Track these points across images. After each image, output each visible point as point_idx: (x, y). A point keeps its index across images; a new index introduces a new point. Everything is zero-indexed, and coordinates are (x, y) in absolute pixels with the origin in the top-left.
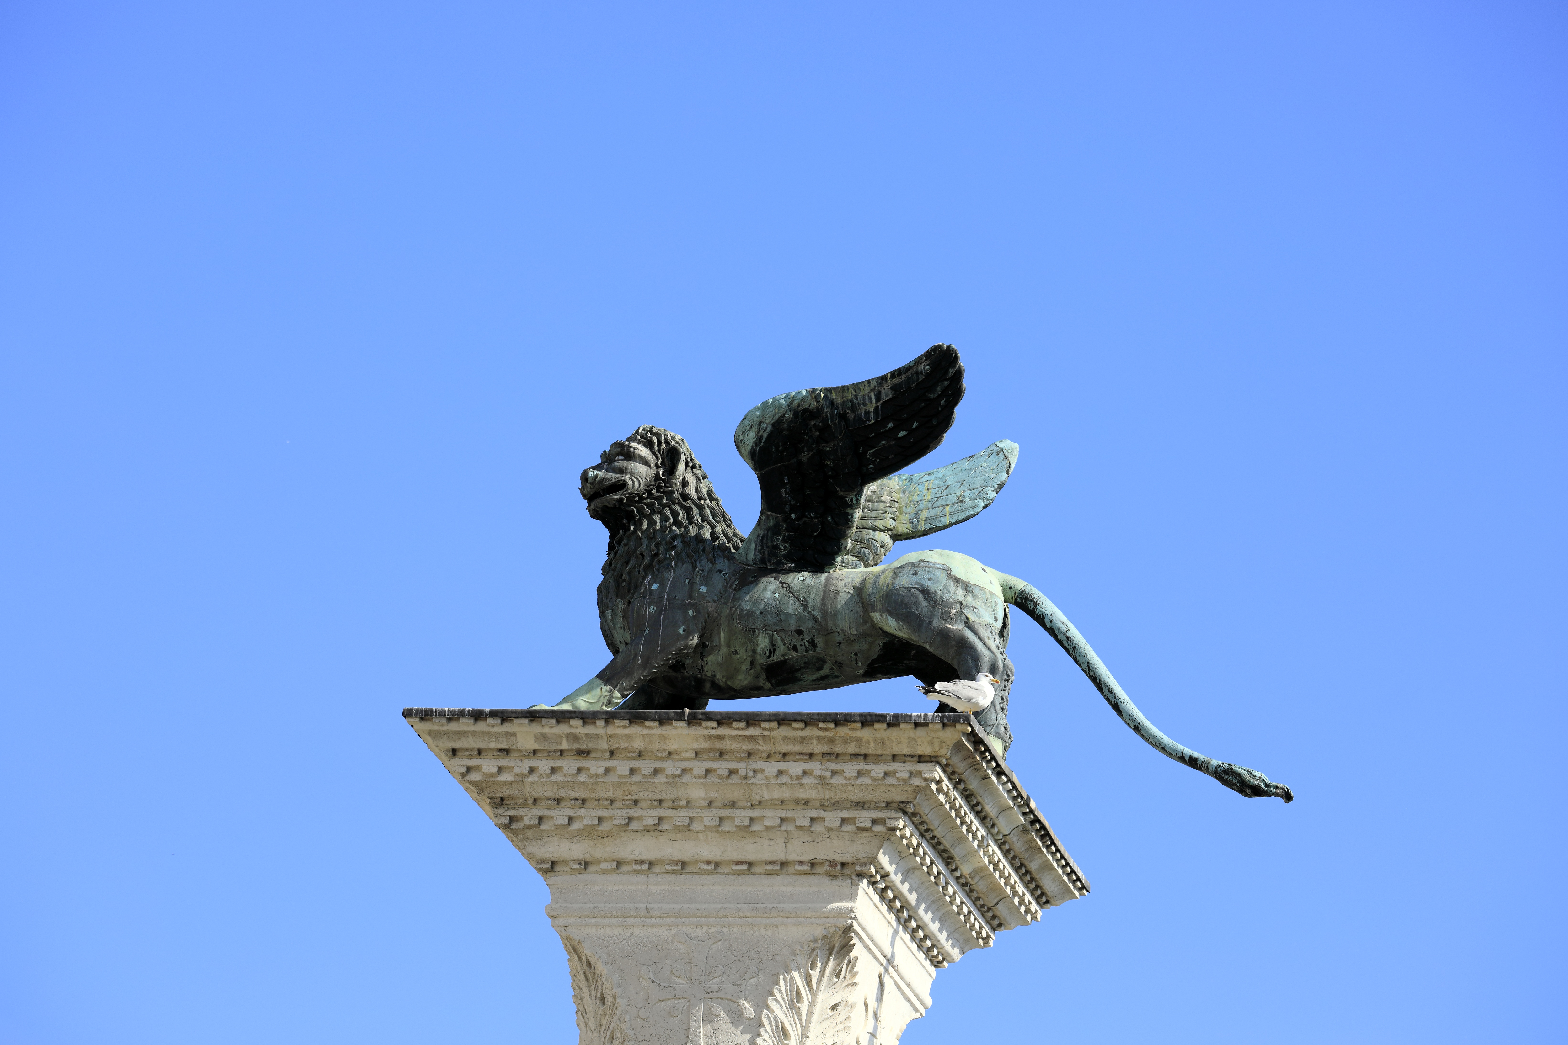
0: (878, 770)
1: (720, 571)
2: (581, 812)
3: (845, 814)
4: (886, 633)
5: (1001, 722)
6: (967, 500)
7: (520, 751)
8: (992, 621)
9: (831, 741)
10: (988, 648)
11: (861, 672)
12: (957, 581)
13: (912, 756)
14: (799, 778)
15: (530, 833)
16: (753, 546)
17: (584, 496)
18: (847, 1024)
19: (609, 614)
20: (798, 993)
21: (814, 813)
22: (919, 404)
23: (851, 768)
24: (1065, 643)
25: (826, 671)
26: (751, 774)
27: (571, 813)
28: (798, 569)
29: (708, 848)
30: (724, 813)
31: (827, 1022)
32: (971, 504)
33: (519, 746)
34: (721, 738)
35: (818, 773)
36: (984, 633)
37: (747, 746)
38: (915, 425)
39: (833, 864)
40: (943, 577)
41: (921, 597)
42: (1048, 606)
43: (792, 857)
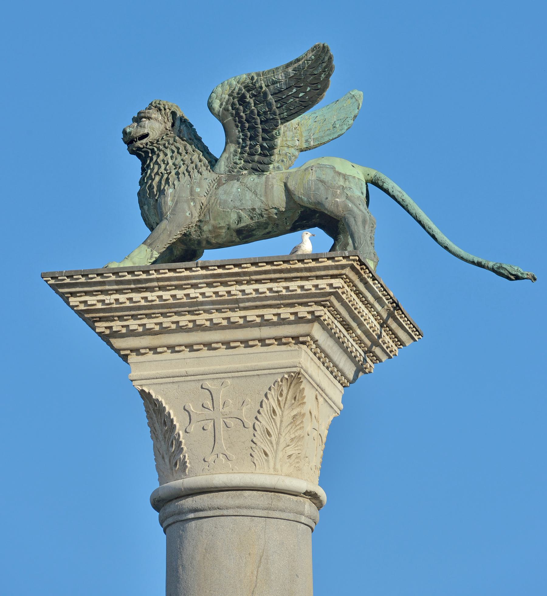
1: (206, 179)
4: (302, 206)
5: (372, 251)
6: (337, 126)
8: (361, 195)
10: (360, 210)
11: (289, 228)
12: (339, 174)
17: (125, 143)
18: (301, 425)
19: (146, 207)
20: (274, 411)
24: (402, 203)
25: (269, 229)
28: (250, 174)
31: (291, 425)
32: (340, 128)
36: (358, 202)
38: (308, 89)
40: (331, 173)
41: (320, 185)
42: (390, 184)
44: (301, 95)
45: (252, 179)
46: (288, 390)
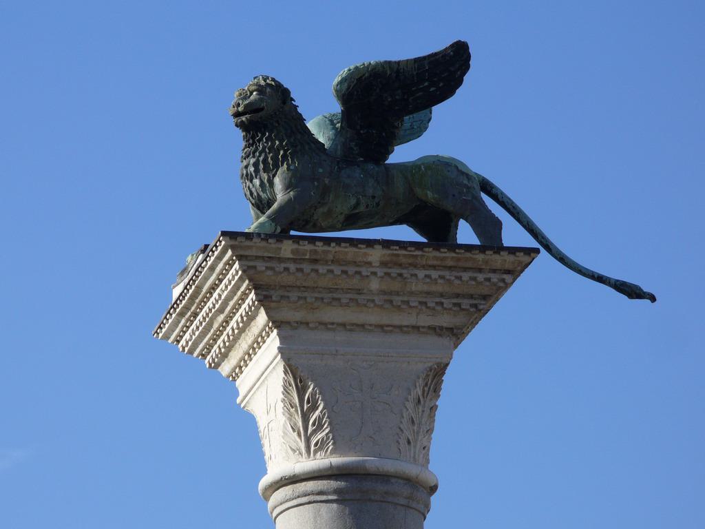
0: (481, 277)
2: (306, 294)
3: (455, 301)
6: (415, 127)
7: (279, 258)
9: (459, 260)
11: (391, 221)
12: (463, 173)
13: (501, 270)
14: (436, 280)
15: (273, 305)
16: (339, 147)
21: (438, 300)
22: (445, 71)
23: (466, 276)
24: (512, 210)
26: (409, 276)
27: (300, 294)
29: (372, 317)
30: (386, 297)
33: (281, 255)
34: (398, 255)
35: (448, 277)
37: (410, 261)
38: (441, 84)
39: (441, 328)
43: (421, 323)
44: (432, 89)
45: (371, 166)
46: (432, 382)
